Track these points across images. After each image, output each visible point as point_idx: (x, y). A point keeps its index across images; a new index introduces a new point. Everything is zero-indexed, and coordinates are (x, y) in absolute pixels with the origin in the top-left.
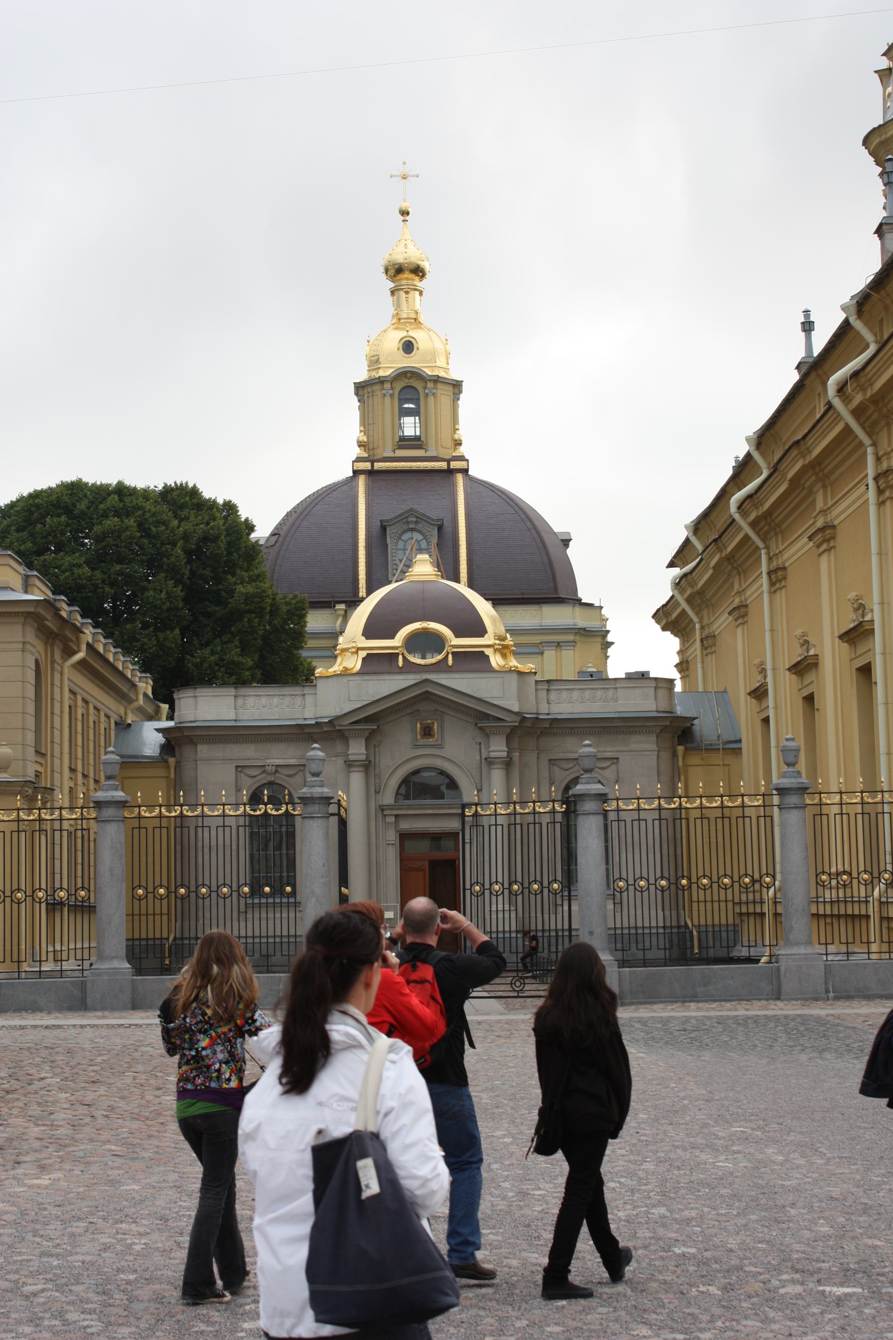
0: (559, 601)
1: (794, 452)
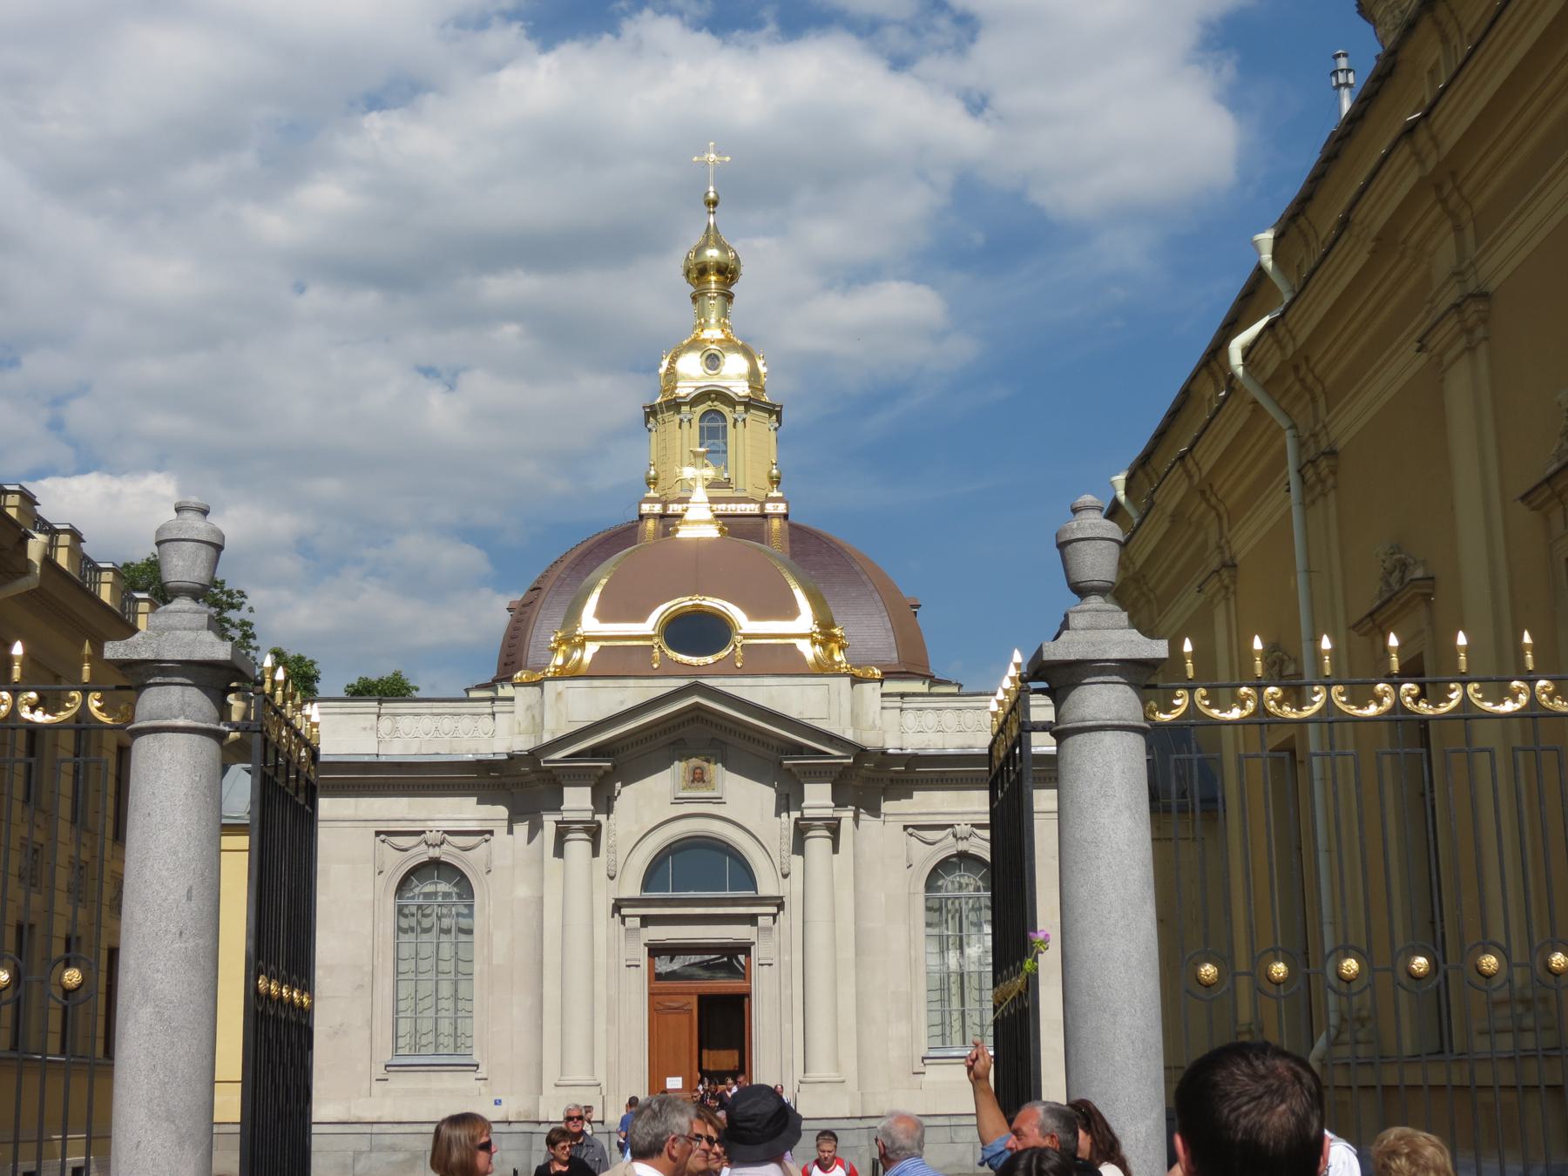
1: (1405, 151)
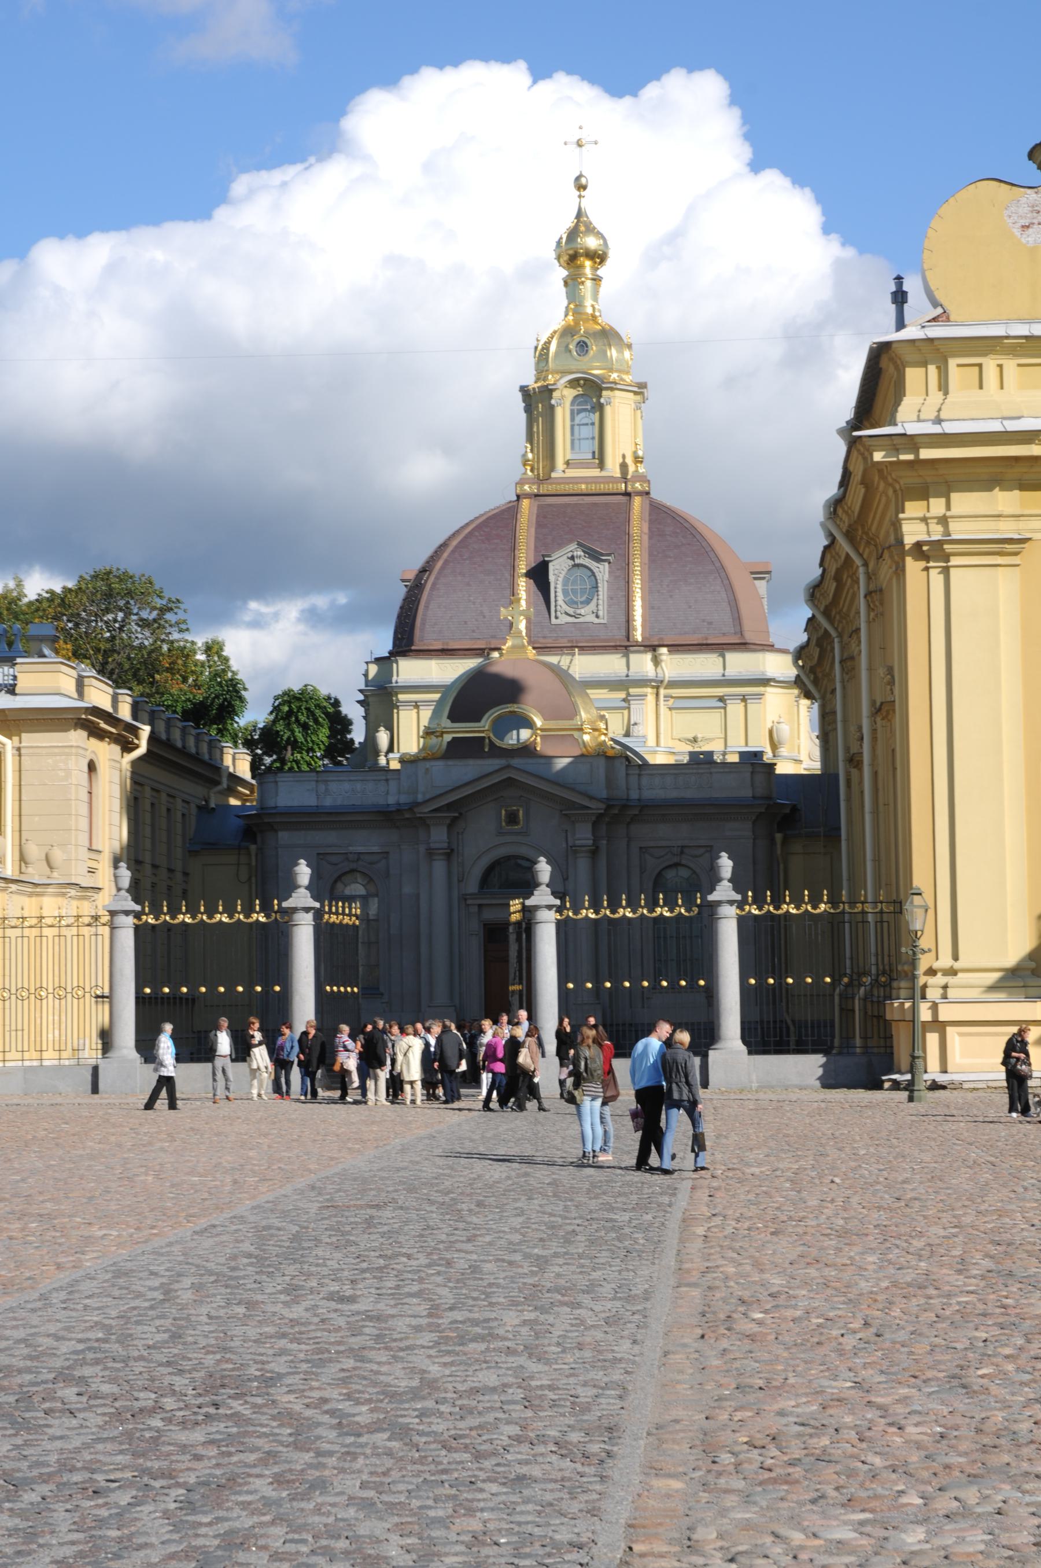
0: (743, 646)
